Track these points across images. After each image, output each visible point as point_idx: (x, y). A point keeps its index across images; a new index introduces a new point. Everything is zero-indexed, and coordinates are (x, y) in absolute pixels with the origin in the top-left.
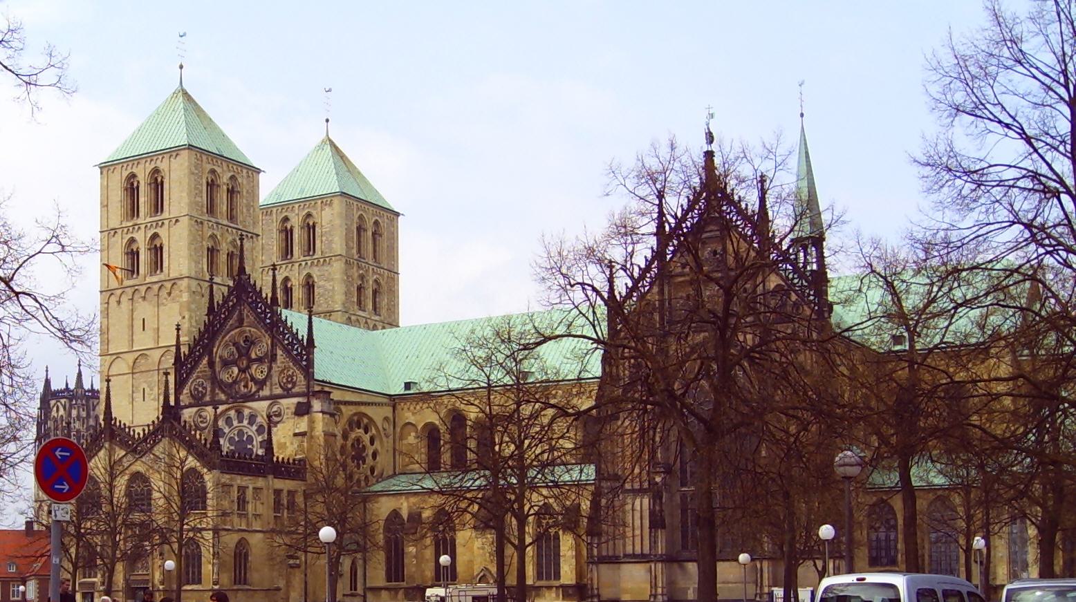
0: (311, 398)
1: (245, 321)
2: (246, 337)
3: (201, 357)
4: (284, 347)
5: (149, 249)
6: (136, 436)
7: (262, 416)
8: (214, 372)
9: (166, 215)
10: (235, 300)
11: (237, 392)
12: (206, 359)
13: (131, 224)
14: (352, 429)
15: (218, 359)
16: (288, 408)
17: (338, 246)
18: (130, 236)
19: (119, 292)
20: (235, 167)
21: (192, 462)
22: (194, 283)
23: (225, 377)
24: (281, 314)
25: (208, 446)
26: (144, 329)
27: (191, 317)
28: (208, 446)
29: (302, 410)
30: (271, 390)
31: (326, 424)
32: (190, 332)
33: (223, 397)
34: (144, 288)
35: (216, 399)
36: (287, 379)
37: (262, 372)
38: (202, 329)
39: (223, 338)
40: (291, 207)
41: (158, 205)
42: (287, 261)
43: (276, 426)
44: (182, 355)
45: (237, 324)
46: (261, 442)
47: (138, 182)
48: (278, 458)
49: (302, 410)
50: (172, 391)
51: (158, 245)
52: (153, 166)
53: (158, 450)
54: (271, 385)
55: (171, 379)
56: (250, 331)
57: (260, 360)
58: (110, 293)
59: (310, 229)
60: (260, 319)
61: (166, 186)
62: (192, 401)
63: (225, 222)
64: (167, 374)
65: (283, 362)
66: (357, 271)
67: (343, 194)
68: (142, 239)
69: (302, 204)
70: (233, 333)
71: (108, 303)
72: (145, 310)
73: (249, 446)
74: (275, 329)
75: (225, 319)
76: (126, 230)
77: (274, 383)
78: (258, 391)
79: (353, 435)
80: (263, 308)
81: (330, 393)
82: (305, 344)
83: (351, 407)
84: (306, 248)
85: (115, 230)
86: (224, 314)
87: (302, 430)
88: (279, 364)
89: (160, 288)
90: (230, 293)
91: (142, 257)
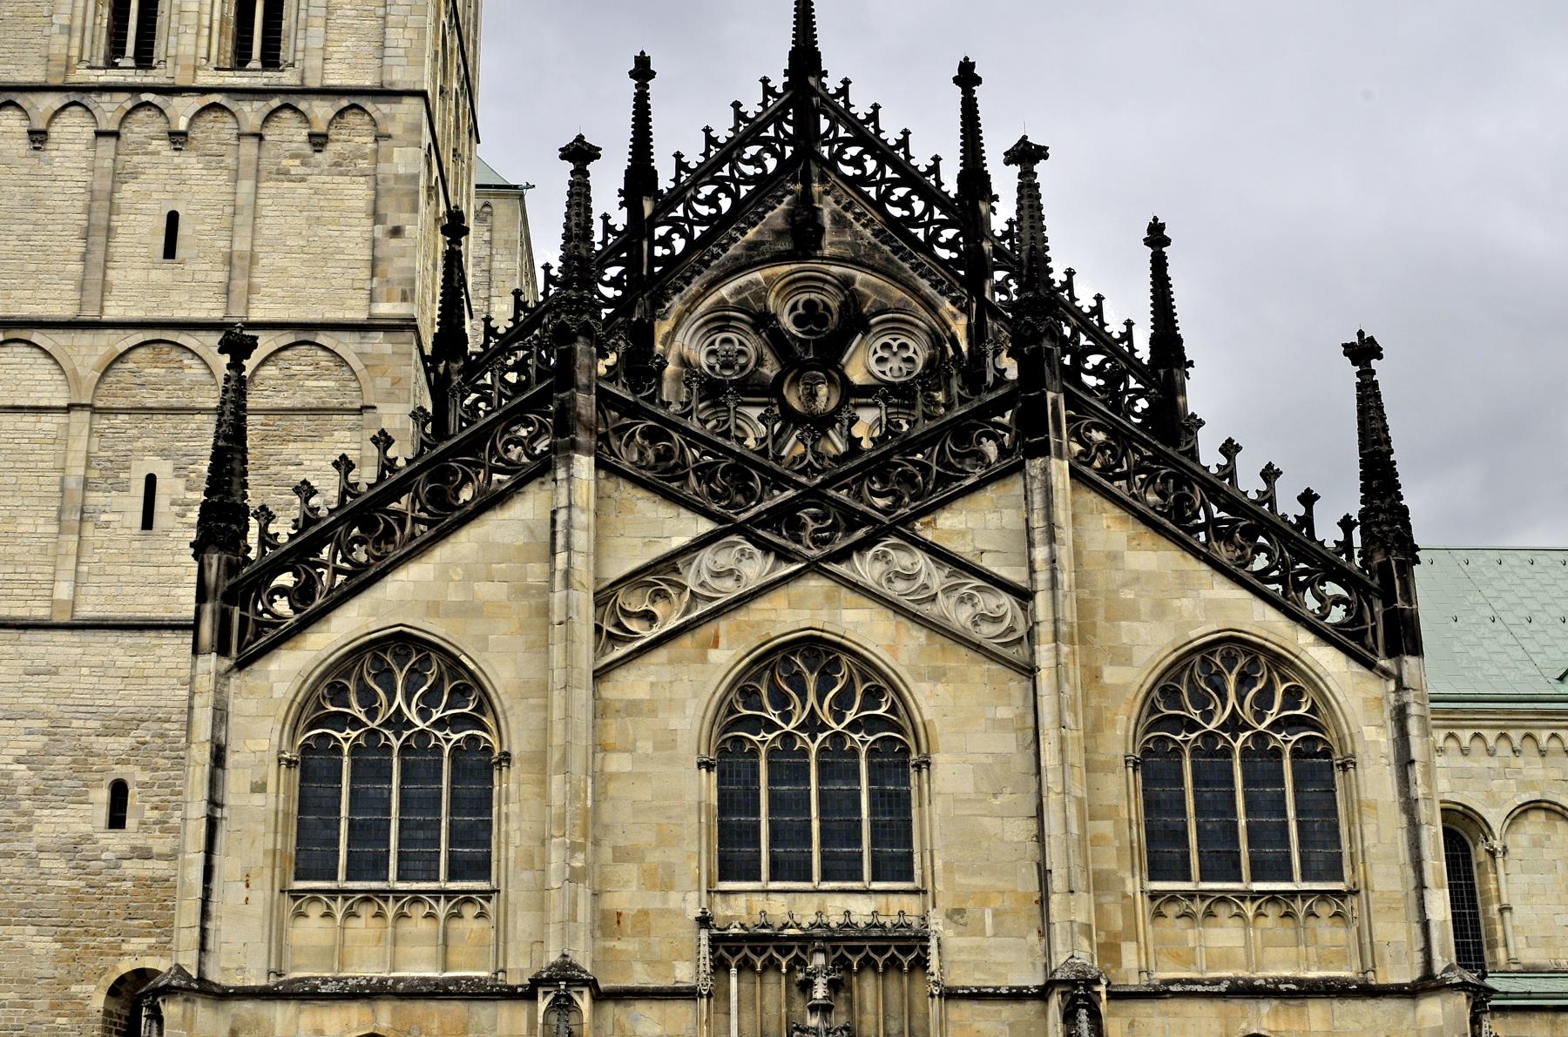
1: (828, 238)
2: (809, 304)
19: (53, 101)
39: (713, 283)
56: (846, 282)
70: (758, 275)
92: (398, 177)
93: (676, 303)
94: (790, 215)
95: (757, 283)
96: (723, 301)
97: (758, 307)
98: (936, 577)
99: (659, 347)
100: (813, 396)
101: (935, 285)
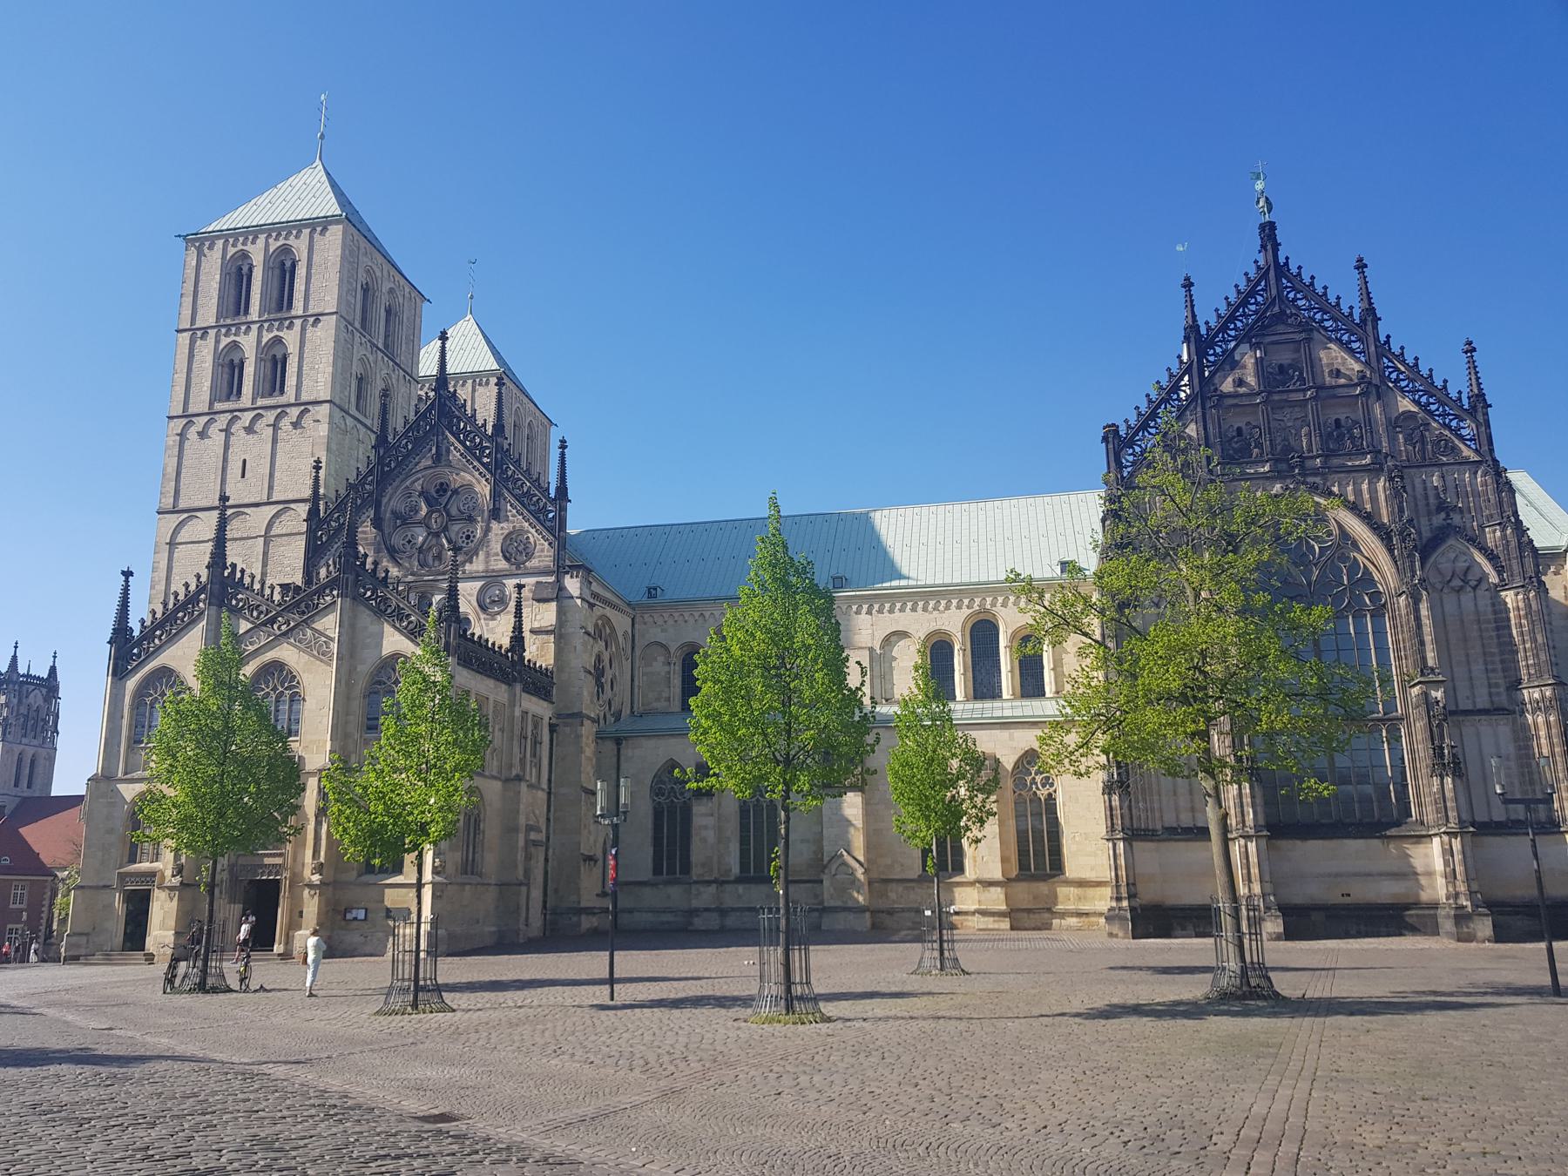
22: (338, 414)
26: (243, 476)
34: (251, 414)
37: (468, 537)
38: (363, 470)
39: (403, 481)
54: (488, 555)
58: (184, 421)
60: (474, 452)
61: (301, 272)
63: (380, 346)
76: (223, 330)
80: (478, 440)
82: (552, 495)
85: (205, 330)
87: (544, 624)
89: (278, 418)
91: (249, 370)
101: (480, 474)
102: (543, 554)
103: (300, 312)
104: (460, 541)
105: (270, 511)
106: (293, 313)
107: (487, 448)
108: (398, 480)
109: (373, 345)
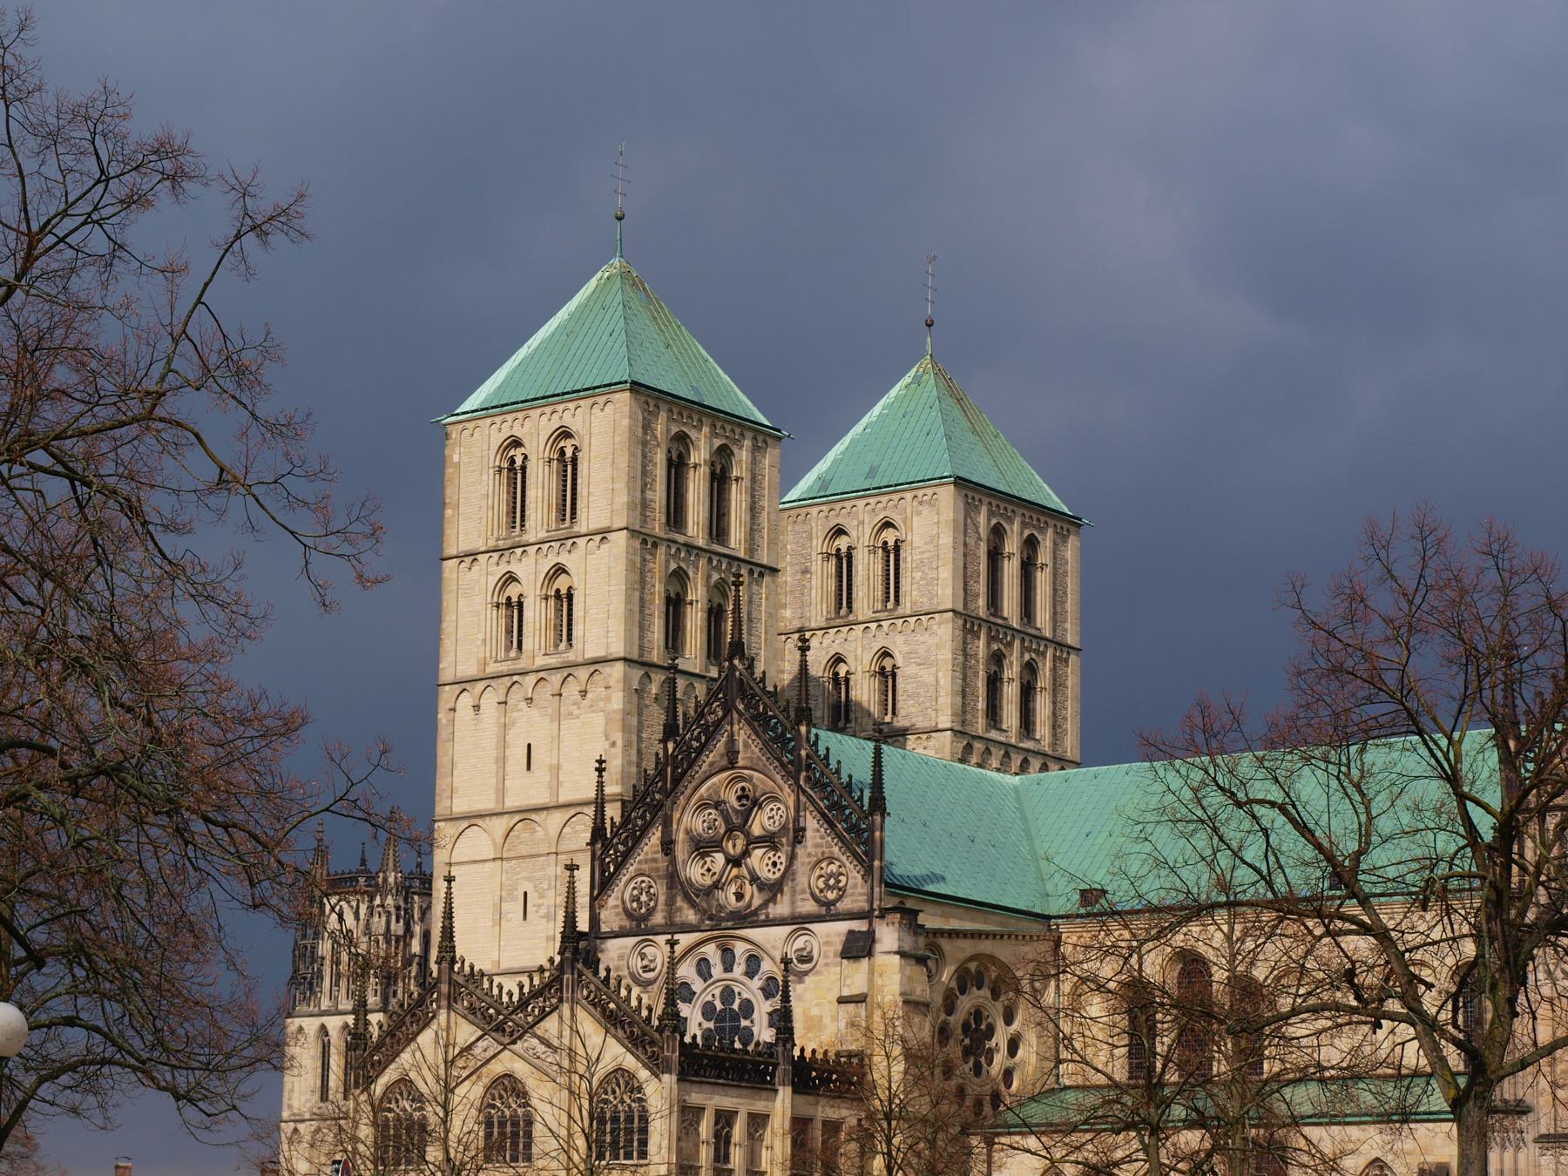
0: (876, 922)
1: (740, 756)
2: (743, 789)
3: (645, 829)
4: (823, 815)
5: (546, 599)
6: (505, 999)
7: (773, 960)
8: (673, 862)
9: (582, 526)
10: (720, 713)
11: (721, 907)
12: (659, 834)
13: (509, 543)
14: (963, 991)
15: (681, 837)
16: (827, 943)
17: (946, 592)
18: (504, 568)
19: (480, 686)
20: (728, 428)
21: (617, 1054)
22: (637, 673)
23: (695, 872)
24: (816, 743)
25: (655, 1023)
26: (529, 767)
27: (627, 745)
28: (655, 1023)
29: (858, 948)
30: (793, 903)
31: (907, 980)
32: (624, 775)
33: (690, 916)
35: (678, 919)
36: (826, 883)
37: (774, 864)
40: (848, 504)
41: (567, 505)
42: (838, 622)
43: (801, 981)
44: (608, 825)
45: (724, 762)
46: (770, 1014)
47: (526, 457)
48: (802, 1050)
49: (858, 948)
50: (583, 899)
51: (564, 591)
52: (555, 423)
53: (550, 1026)
55: (583, 878)
57: (769, 841)
58: (458, 688)
59: (892, 554)
61: (583, 467)
62: (626, 923)
64: (572, 868)
65: (817, 846)
66: (988, 644)
67: (961, 482)
68: (530, 570)
69: (872, 501)
70: (715, 779)
71: (454, 710)
72: (531, 724)
73: (744, 1023)
74: (804, 774)
75: (700, 751)
77: (798, 888)
78: (765, 905)
79: (965, 1004)
81: (915, 913)
82: (865, 808)
83: (961, 943)
84: (879, 594)
85: (473, 555)
86: (698, 739)
88: (810, 849)
90: (712, 695)
91: (527, 614)
92: (614, 711)
93: (682, 800)
94: (726, 744)
95: (714, 784)
96: (701, 798)
97: (716, 799)
98: (541, 1048)
99: (675, 826)
100: (734, 846)
102: (857, 893)
103: (584, 530)
104: (766, 869)
105: (557, 818)
106: (576, 529)
107: (790, 740)
108: (691, 787)
109: (690, 547)
